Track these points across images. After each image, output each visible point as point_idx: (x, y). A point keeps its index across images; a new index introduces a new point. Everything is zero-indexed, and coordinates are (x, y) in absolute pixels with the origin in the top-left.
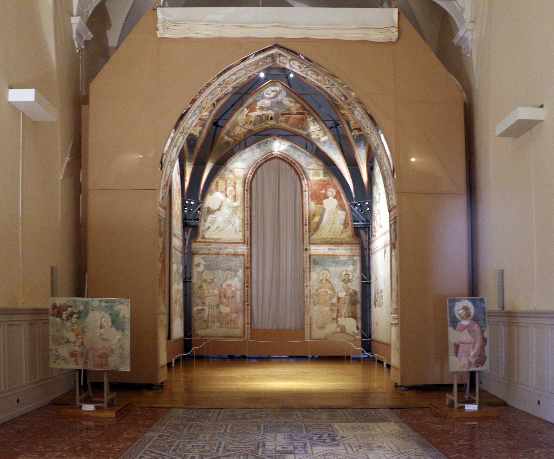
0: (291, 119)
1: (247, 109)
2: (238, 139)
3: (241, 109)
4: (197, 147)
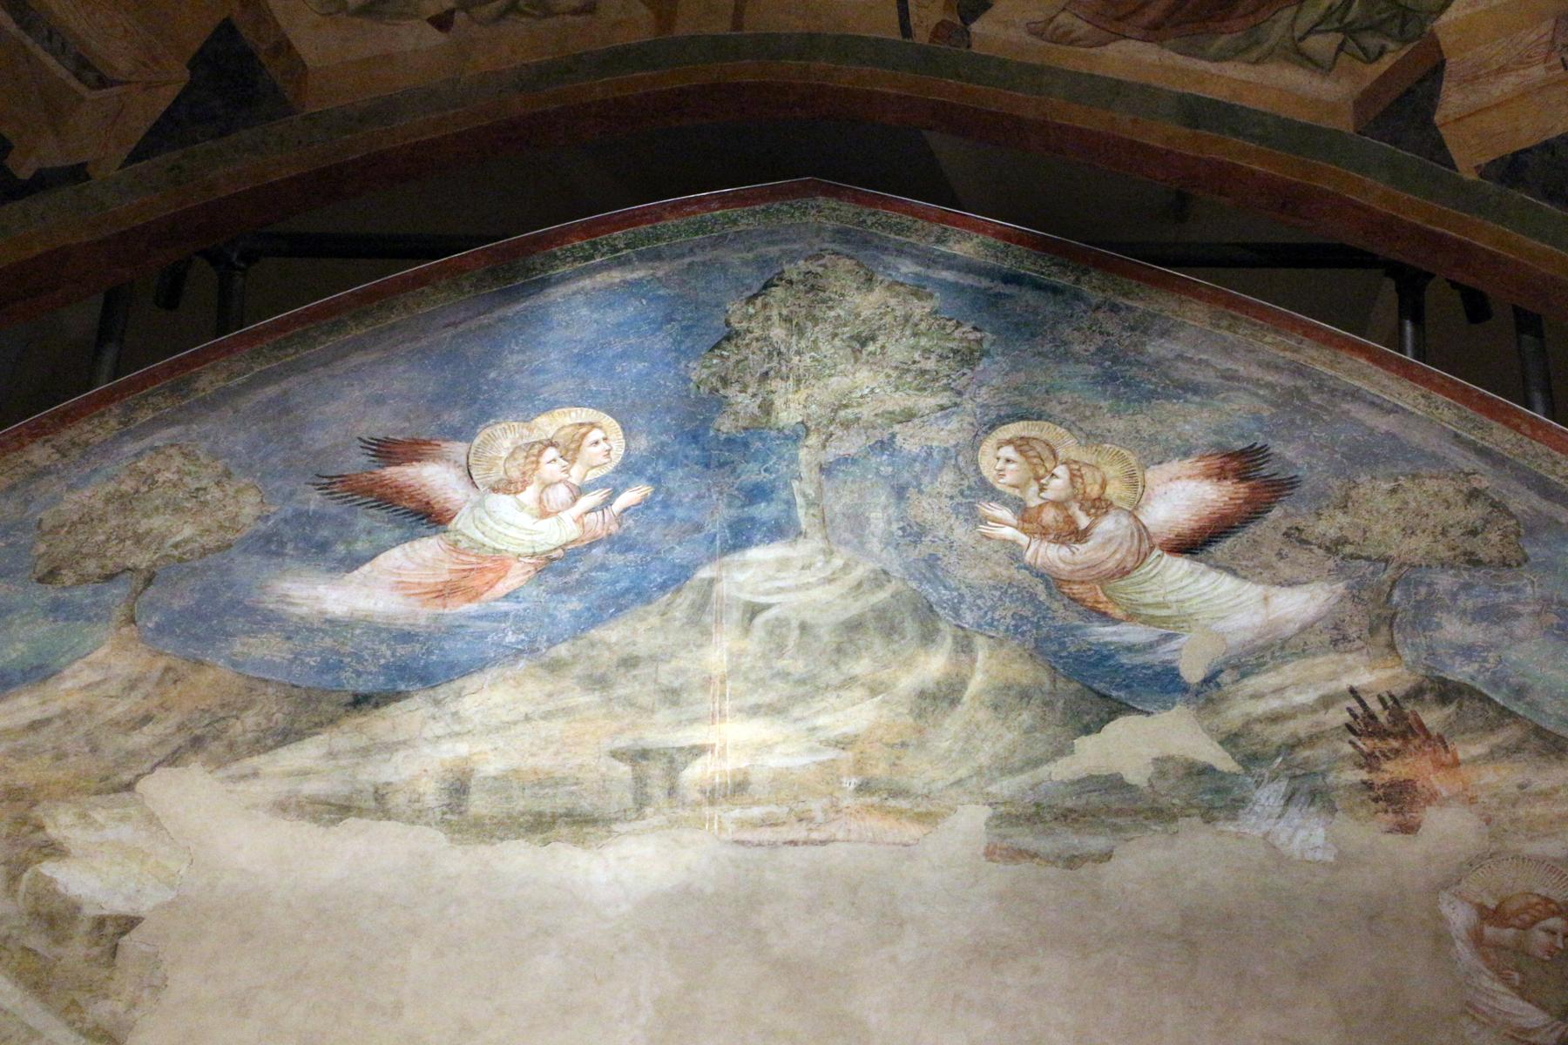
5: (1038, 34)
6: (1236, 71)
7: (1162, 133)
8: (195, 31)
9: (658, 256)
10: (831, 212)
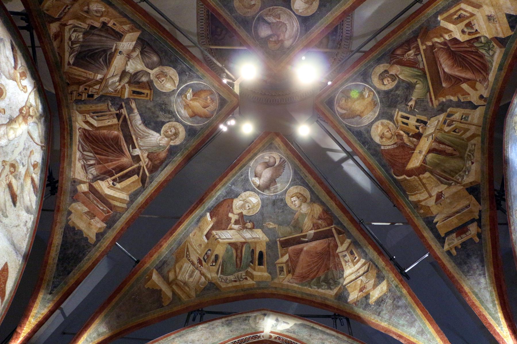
0: (302, 256)
1: (211, 217)
2: (183, 296)
3: (198, 212)
4: (81, 264)
5: (487, 89)
6: (494, 64)
7: (503, 73)
8: (466, 193)
9: (509, 142)
10: (508, 119)
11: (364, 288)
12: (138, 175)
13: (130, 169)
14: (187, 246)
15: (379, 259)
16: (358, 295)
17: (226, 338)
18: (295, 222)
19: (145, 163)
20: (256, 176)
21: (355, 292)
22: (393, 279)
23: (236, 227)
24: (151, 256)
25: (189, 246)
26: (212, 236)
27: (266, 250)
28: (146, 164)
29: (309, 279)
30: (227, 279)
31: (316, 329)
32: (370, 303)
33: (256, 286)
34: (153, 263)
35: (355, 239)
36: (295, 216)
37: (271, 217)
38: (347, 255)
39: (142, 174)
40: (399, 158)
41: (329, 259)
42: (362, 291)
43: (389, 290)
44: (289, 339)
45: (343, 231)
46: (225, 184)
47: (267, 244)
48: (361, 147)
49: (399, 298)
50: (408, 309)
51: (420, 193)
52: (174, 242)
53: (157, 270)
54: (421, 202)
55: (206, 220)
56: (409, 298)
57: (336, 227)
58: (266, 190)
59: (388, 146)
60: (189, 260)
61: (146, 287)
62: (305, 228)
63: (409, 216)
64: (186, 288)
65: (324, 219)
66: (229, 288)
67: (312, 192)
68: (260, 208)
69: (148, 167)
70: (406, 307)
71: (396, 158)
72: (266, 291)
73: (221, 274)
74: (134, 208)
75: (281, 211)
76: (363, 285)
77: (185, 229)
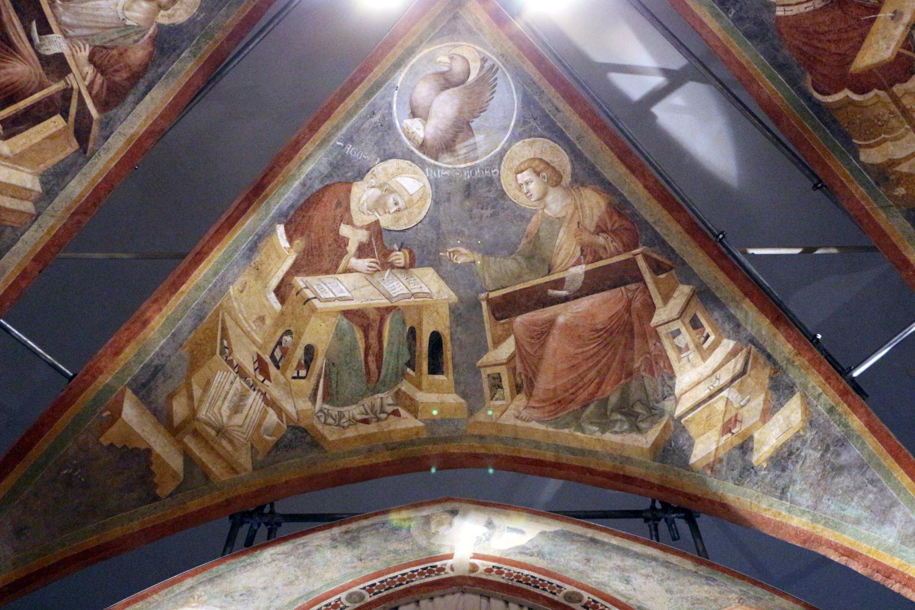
0: (554, 342)
1: (290, 239)
2: (216, 469)
3: (250, 224)
11: (736, 421)
12: (65, 115)
13: (37, 97)
14: (223, 321)
15: (775, 335)
16: (718, 442)
17: (345, 576)
18: (530, 242)
19: (84, 79)
20: (414, 115)
21: (709, 434)
22: (820, 390)
23: (363, 264)
24: (117, 354)
25: (230, 323)
26: (294, 292)
27: (451, 328)
28: (87, 83)
29: (574, 407)
30: (341, 415)
31: (603, 544)
32: (756, 464)
33: (424, 435)
34: (123, 370)
35: (703, 283)
36: (531, 227)
37: (460, 233)
38: (683, 330)
39: (78, 113)
40: (829, 41)
41: (629, 346)
42: (730, 431)
43: (811, 423)
44: (526, 572)
45: (669, 263)
46: (324, 142)
47: (453, 310)
48: (717, 16)
49: (841, 443)
50: (868, 475)
51: (896, 139)
52: (184, 311)
53: (136, 392)
54: (899, 164)
55: (276, 247)
56: (871, 442)
57: (649, 253)
58: (445, 155)
59: (797, 4)
60: (230, 363)
61: (105, 441)
62: (559, 261)
63: (863, 208)
64: (224, 443)
65: (613, 232)
66: (346, 440)
67: (576, 155)
68: (428, 206)
69: (94, 92)
70: (862, 467)
71: (820, 41)
72: (453, 449)
73: (324, 400)
74: (59, 213)
75: (488, 212)
76: (733, 413)
77: (216, 274)
